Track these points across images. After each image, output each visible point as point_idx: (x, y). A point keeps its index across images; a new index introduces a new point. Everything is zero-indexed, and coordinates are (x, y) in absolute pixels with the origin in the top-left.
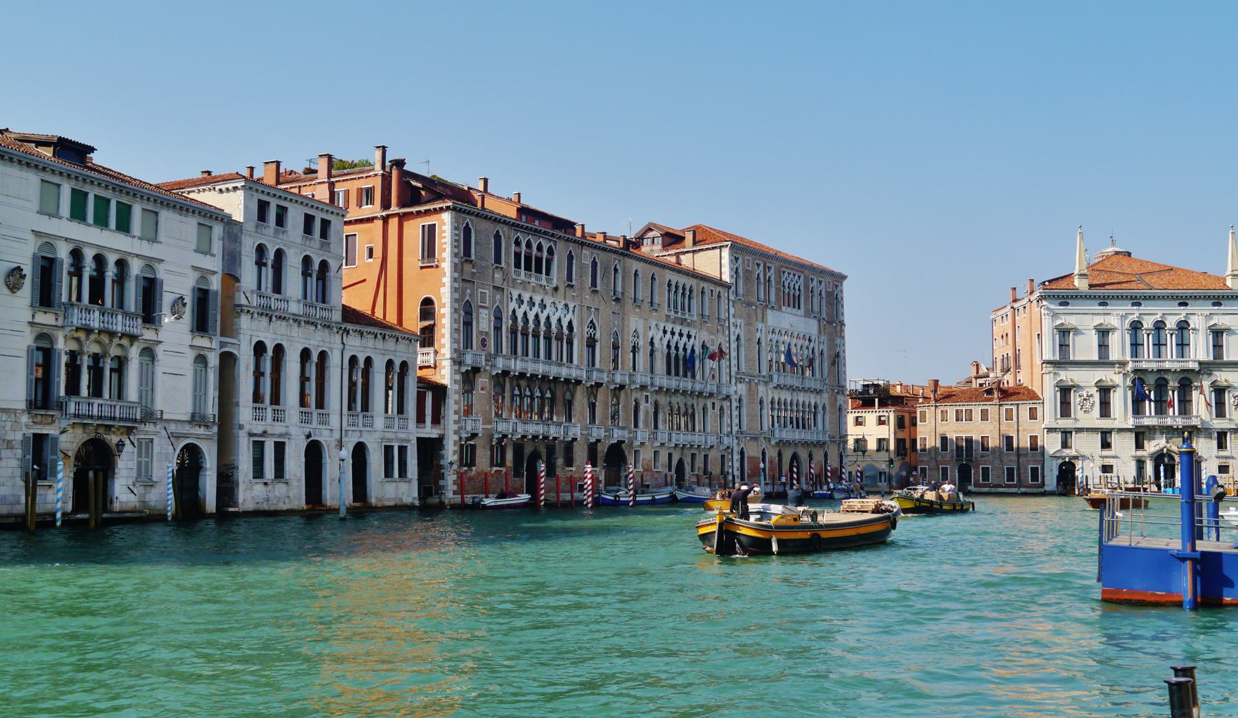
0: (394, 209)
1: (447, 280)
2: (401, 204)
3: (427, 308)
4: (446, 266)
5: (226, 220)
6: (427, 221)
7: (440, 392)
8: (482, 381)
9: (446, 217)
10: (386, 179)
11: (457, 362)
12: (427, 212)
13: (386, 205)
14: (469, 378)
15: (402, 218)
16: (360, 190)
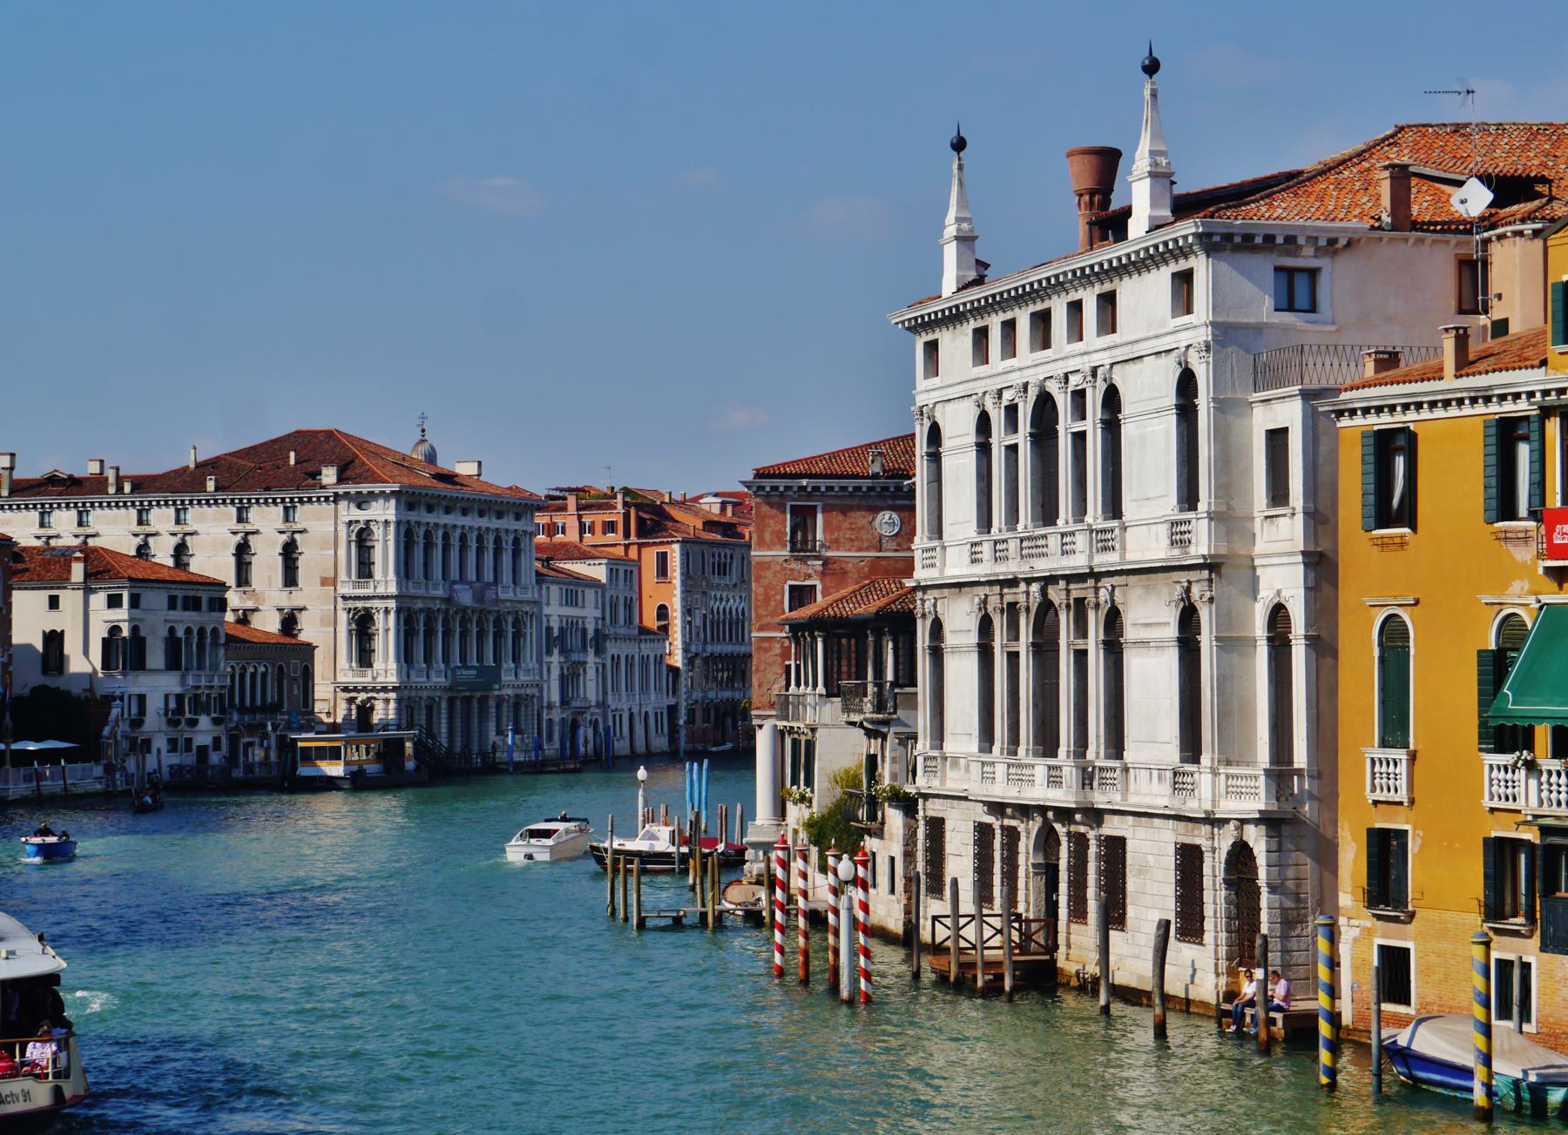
0: (633, 539)
1: (678, 592)
2: (639, 535)
3: (663, 612)
4: (677, 582)
5: (593, 583)
6: (661, 549)
7: (674, 671)
8: (698, 662)
9: (676, 547)
10: (627, 517)
11: (686, 650)
12: (662, 543)
13: (627, 535)
14: (690, 661)
15: (641, 546)
16: (604, 523)
